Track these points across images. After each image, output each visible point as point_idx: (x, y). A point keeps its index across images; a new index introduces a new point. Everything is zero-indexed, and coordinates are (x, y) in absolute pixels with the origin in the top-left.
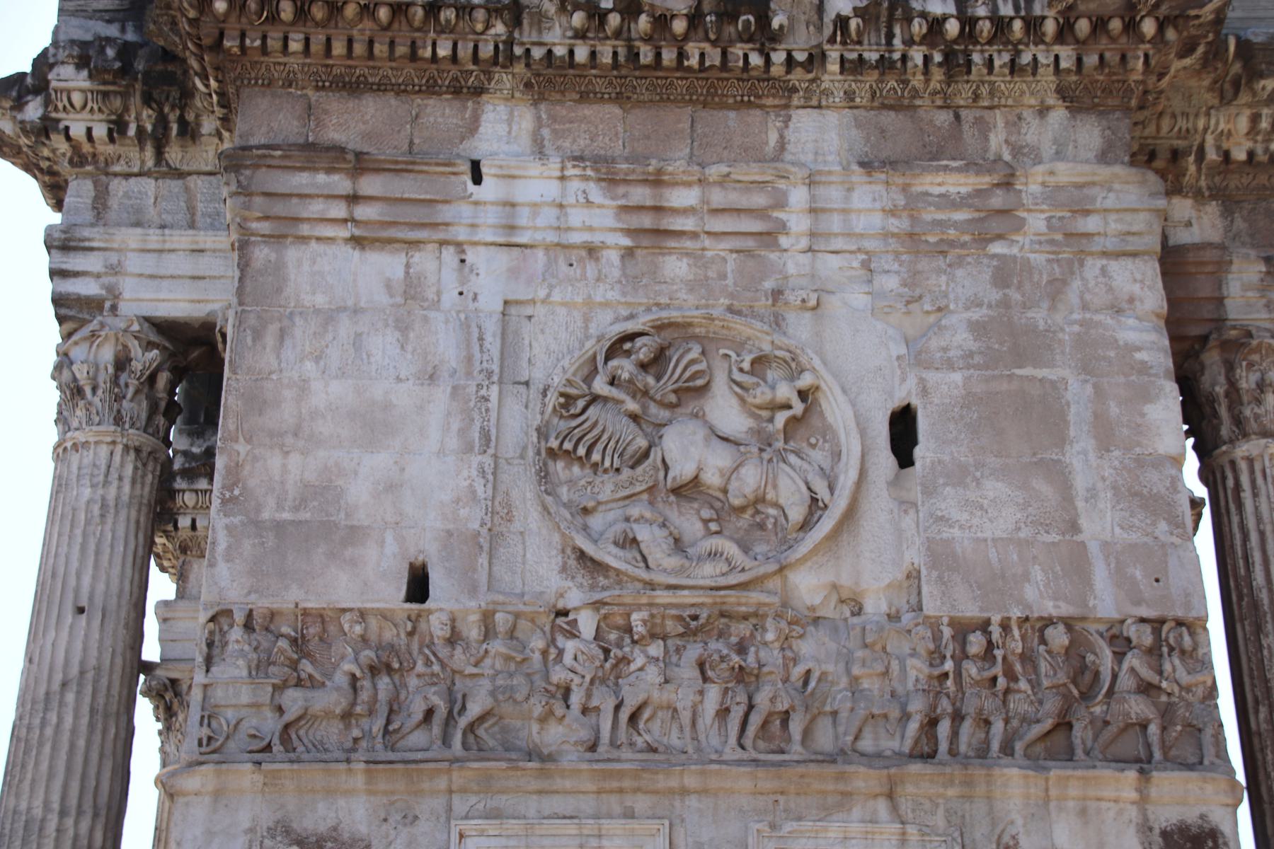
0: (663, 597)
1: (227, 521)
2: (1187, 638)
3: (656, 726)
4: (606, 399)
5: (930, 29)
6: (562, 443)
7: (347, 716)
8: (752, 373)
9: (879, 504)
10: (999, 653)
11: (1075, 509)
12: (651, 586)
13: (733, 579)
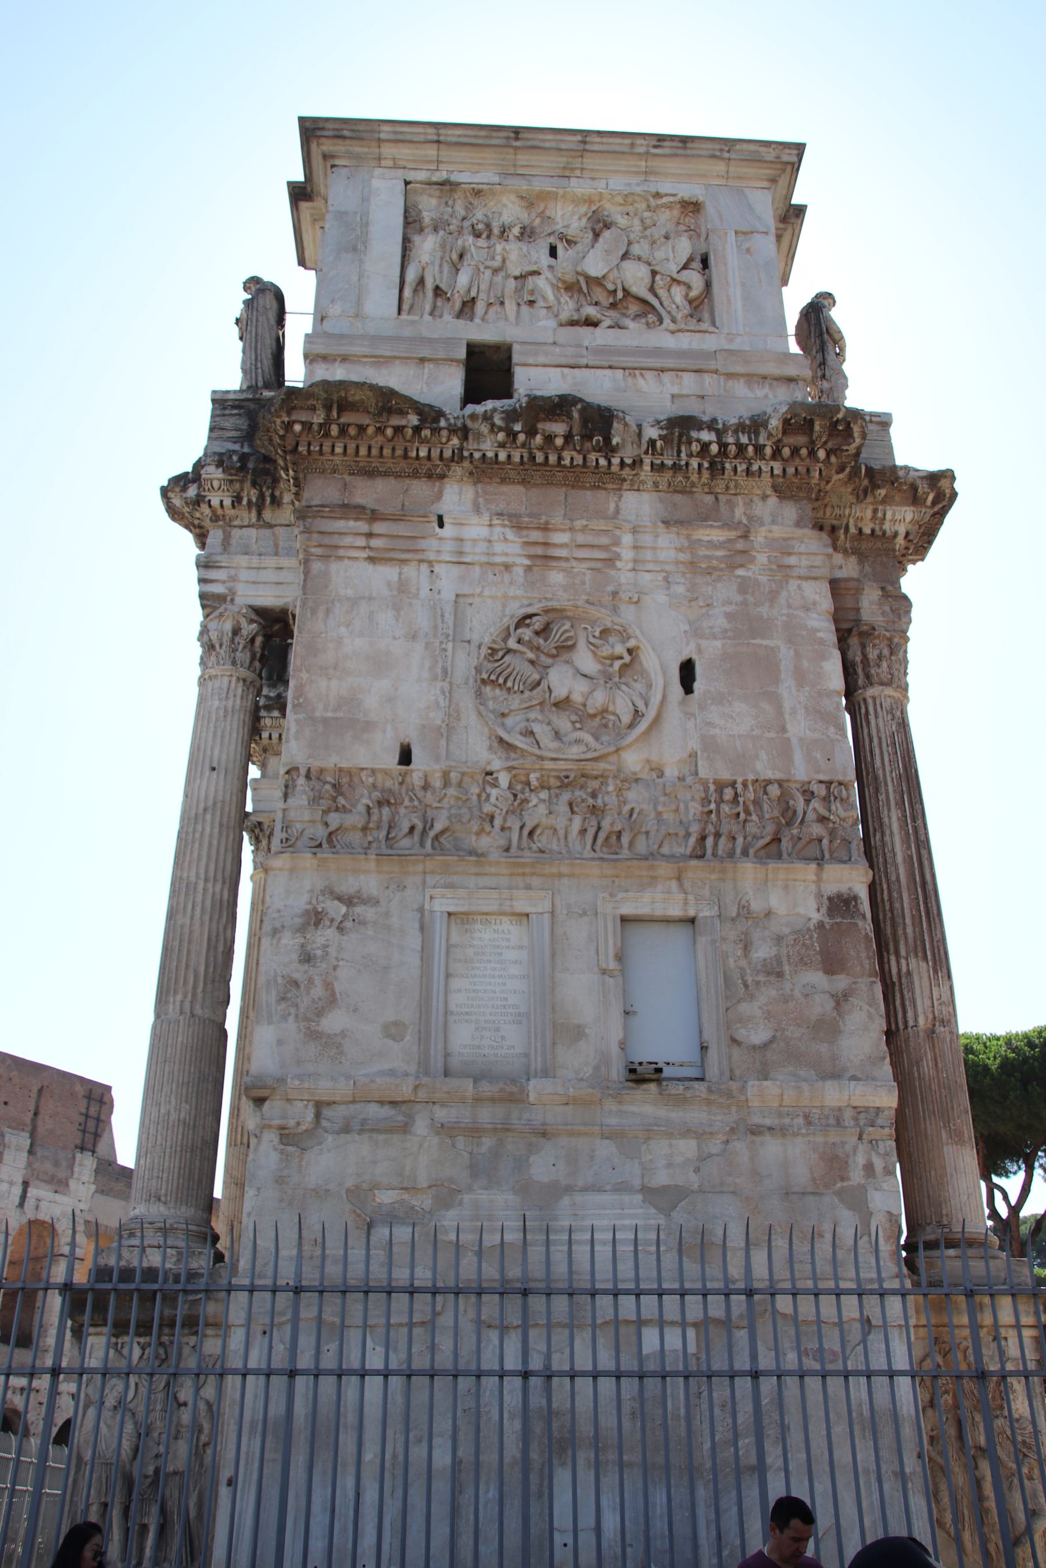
1: (296, 717)
2: (844, 792)
3: (544, 839)
4: (515, 651)
5: (702, 448)
7: (365, 829)
8: (600, 638)
9: (674, 715)
10: (741, 800)
12: (542, 758)
13: (589, 756)
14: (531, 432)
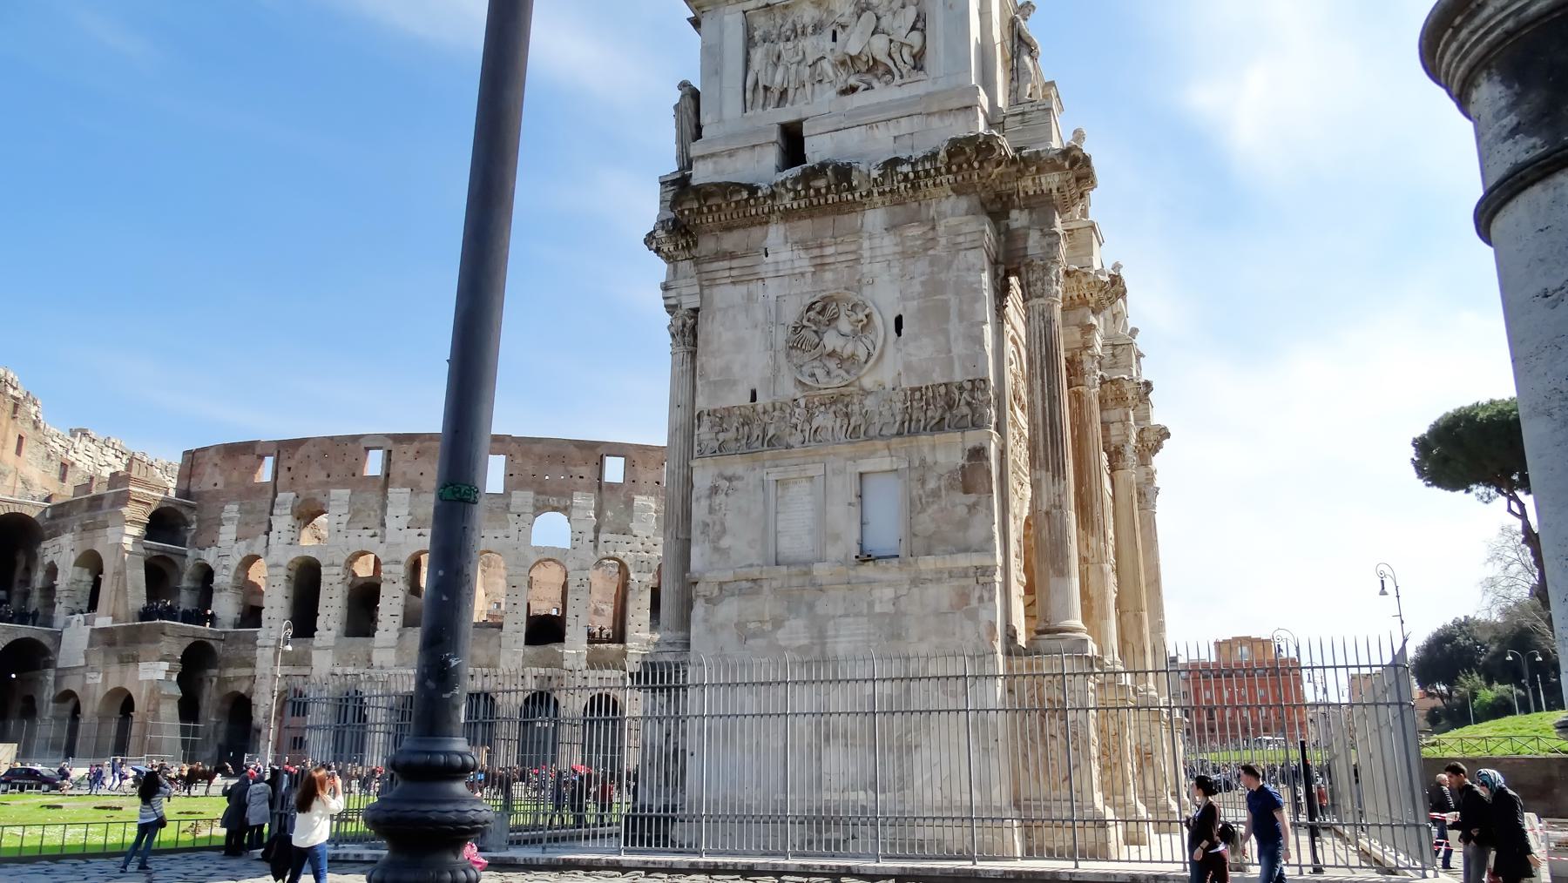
0: (823, 392)
7: (736, 440)
9: (890, 351)
13: (843, 384)
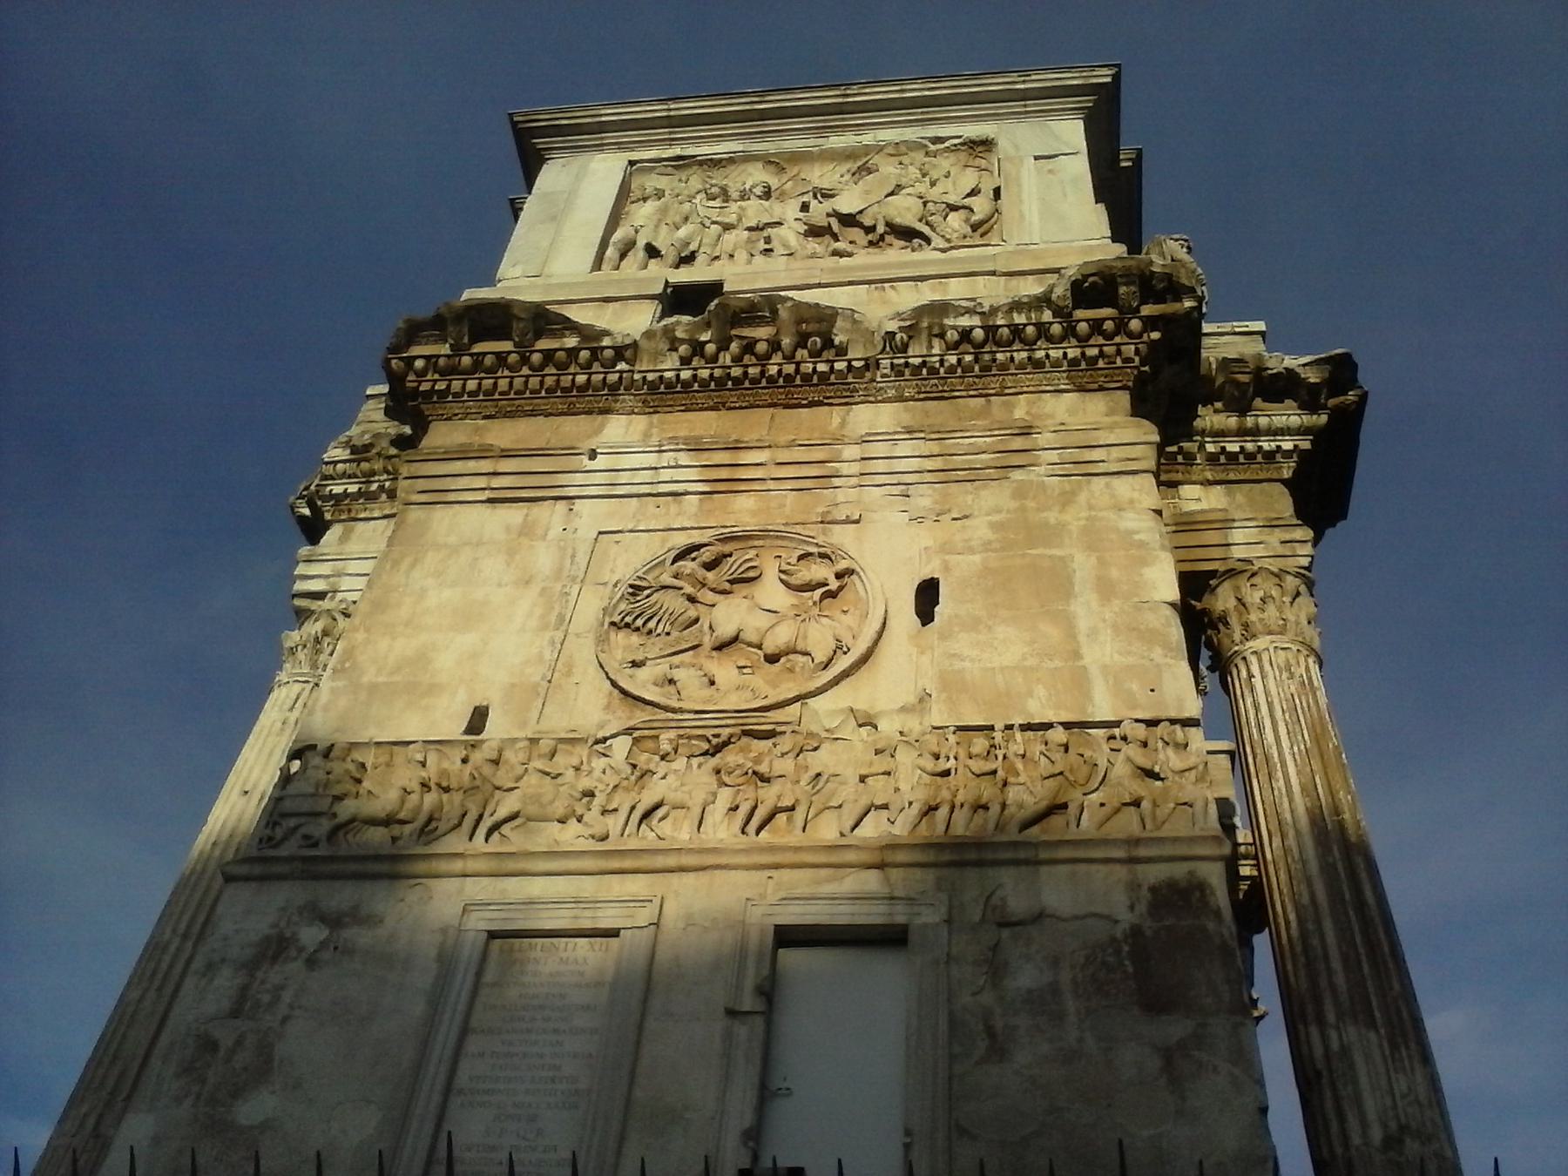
1: (334, 684)
6: (624, 618)
11: (1078, 642)
12: (681, 711)
14: (723, 346)
